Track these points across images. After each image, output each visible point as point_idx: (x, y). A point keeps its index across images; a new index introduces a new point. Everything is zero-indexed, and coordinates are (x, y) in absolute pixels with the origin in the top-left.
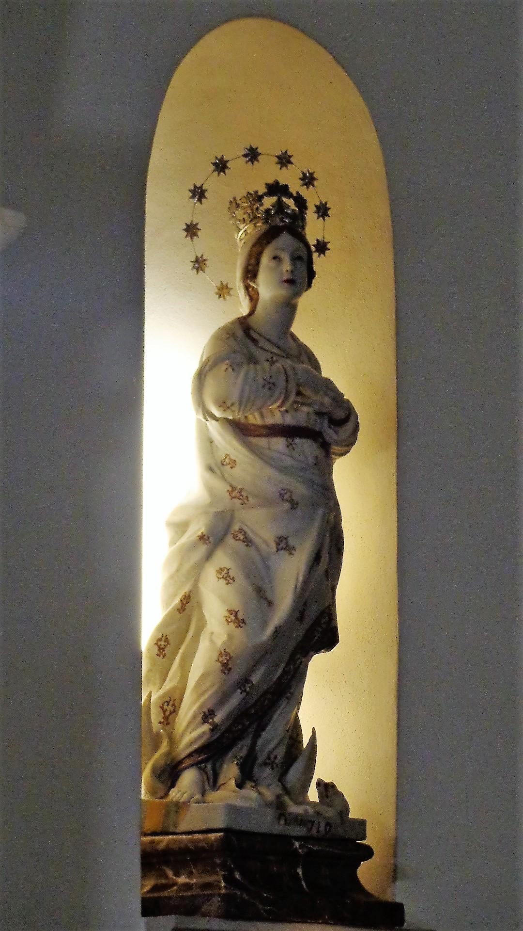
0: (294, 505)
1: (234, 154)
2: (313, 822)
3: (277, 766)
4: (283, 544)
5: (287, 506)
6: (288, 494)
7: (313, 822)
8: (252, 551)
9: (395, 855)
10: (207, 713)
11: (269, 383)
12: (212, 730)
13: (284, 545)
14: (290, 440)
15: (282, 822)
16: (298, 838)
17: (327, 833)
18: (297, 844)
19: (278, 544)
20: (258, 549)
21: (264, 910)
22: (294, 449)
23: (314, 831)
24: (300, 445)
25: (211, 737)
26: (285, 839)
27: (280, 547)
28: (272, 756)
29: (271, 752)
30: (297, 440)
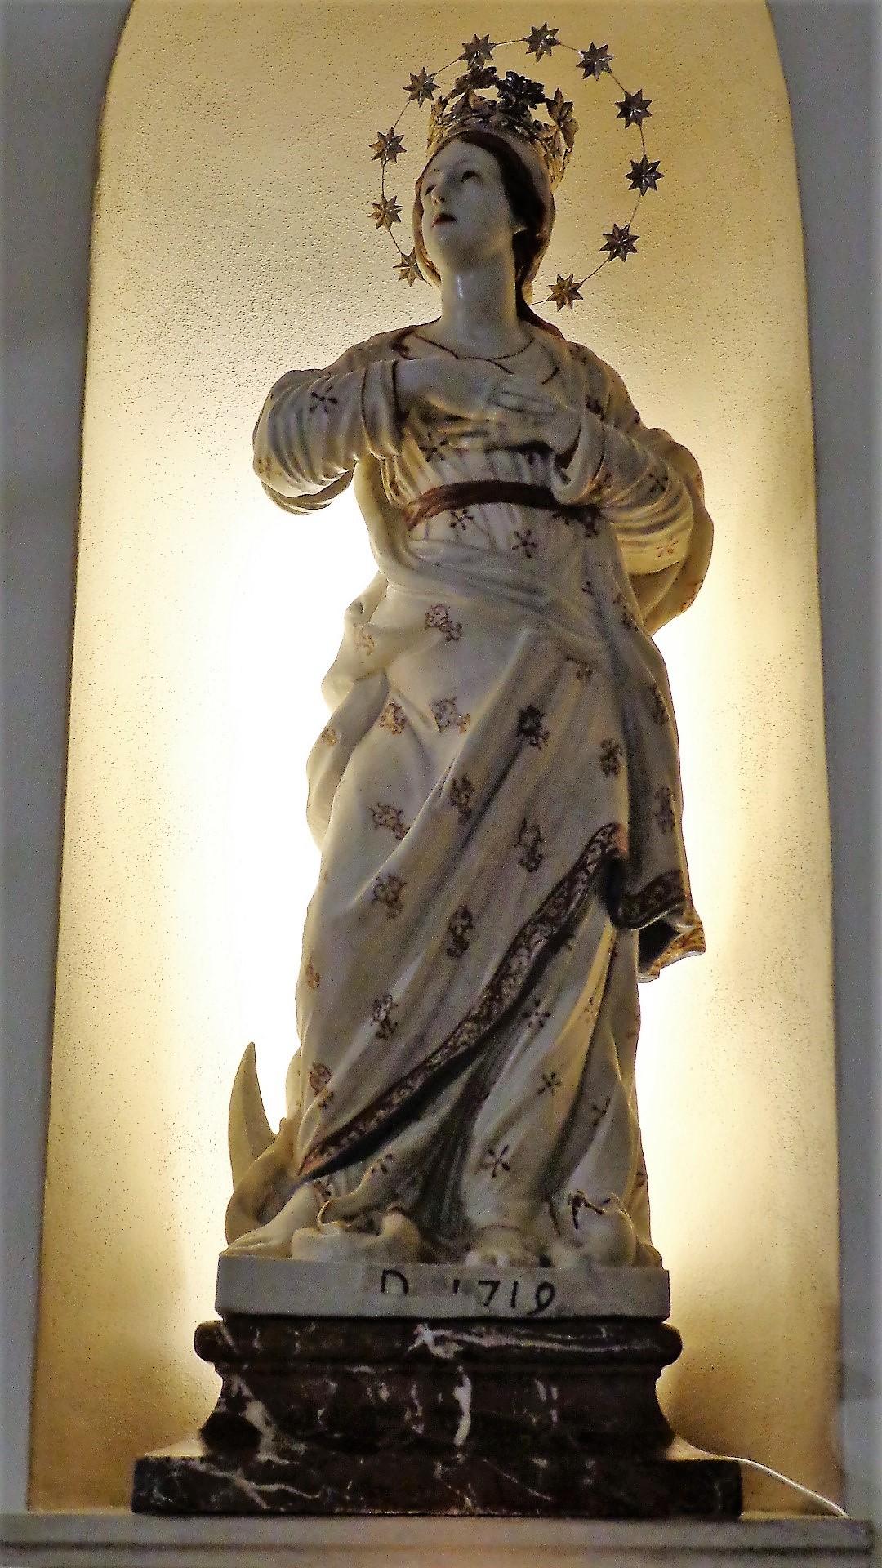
0: (451, 632)
1: (649, 141)
2: (495, 1285)
3: (506, 1167)
4: (446, 715)
5: (437, 636)
6: (443, 614)
7: (495, 1285)
8: (404, 738)
9: (839, 1346)
10: (315, 1072)
11: (323, 399)
12: (324, 1105)
13: (445, 711)
14: (459, 512)
15: (394, 1286)
16: (434, 1323)
17: (541, 1306)
18: (426, 1335)
19: (439, 717)
20: (414, 734)
21: (262, 1494)
22: (464, 528)
23: (501, 1306)
24: (479, 519)
25: (332, 1119)
26: (406, 1325)
27: (443, 722)
28: (499, 1149)
29: (496, 1139)
30: (474, 509)
